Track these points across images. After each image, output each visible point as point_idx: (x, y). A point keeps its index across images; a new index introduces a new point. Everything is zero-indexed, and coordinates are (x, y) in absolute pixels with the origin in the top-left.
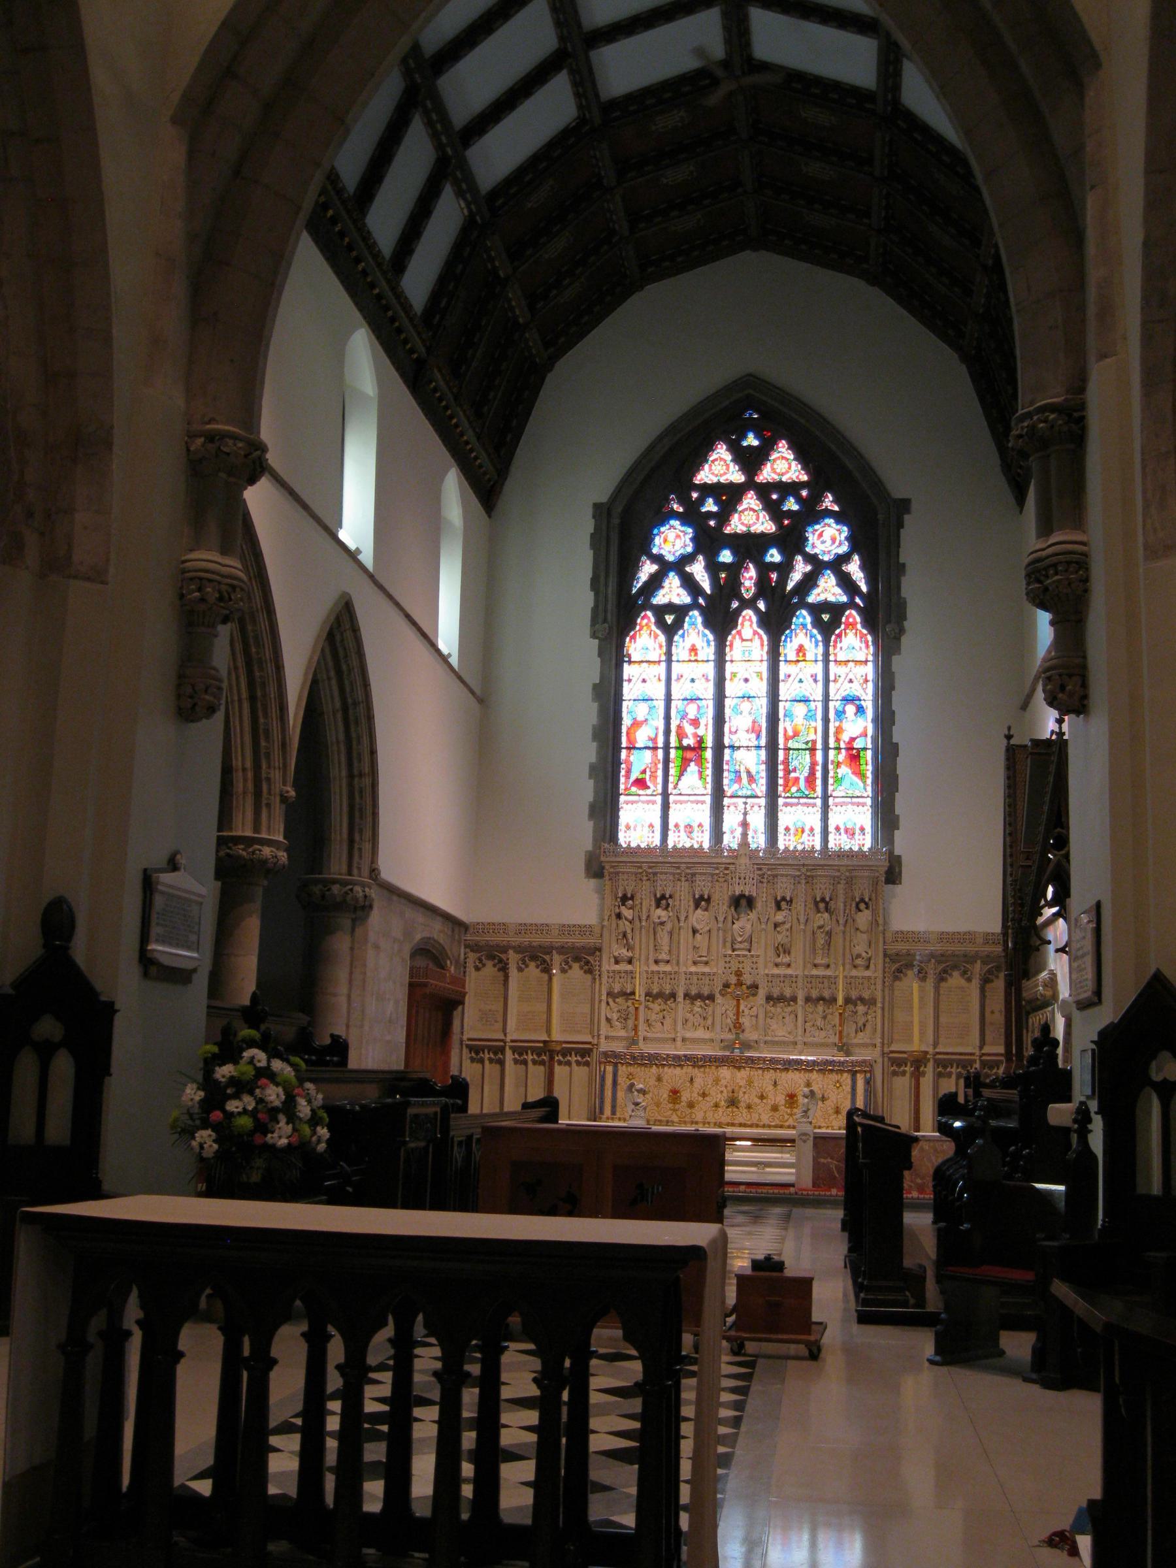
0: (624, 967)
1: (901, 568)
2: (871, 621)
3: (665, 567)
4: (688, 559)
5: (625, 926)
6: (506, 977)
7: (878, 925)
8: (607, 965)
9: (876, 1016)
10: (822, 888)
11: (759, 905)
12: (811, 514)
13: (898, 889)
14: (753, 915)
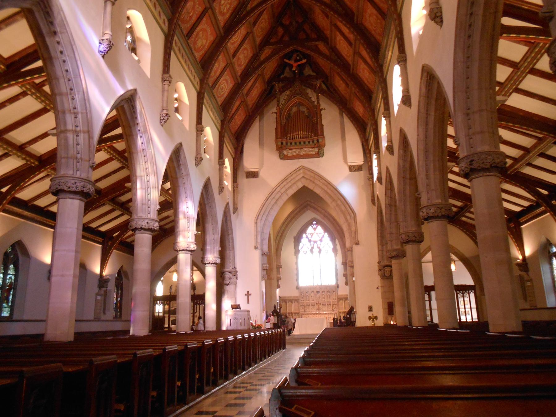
0: (302, 302)
5: (302, 296)
6: (286, 304)
8: (300, 302)
11: (320, 292)
13: (339, 289)
14: (319, 294)
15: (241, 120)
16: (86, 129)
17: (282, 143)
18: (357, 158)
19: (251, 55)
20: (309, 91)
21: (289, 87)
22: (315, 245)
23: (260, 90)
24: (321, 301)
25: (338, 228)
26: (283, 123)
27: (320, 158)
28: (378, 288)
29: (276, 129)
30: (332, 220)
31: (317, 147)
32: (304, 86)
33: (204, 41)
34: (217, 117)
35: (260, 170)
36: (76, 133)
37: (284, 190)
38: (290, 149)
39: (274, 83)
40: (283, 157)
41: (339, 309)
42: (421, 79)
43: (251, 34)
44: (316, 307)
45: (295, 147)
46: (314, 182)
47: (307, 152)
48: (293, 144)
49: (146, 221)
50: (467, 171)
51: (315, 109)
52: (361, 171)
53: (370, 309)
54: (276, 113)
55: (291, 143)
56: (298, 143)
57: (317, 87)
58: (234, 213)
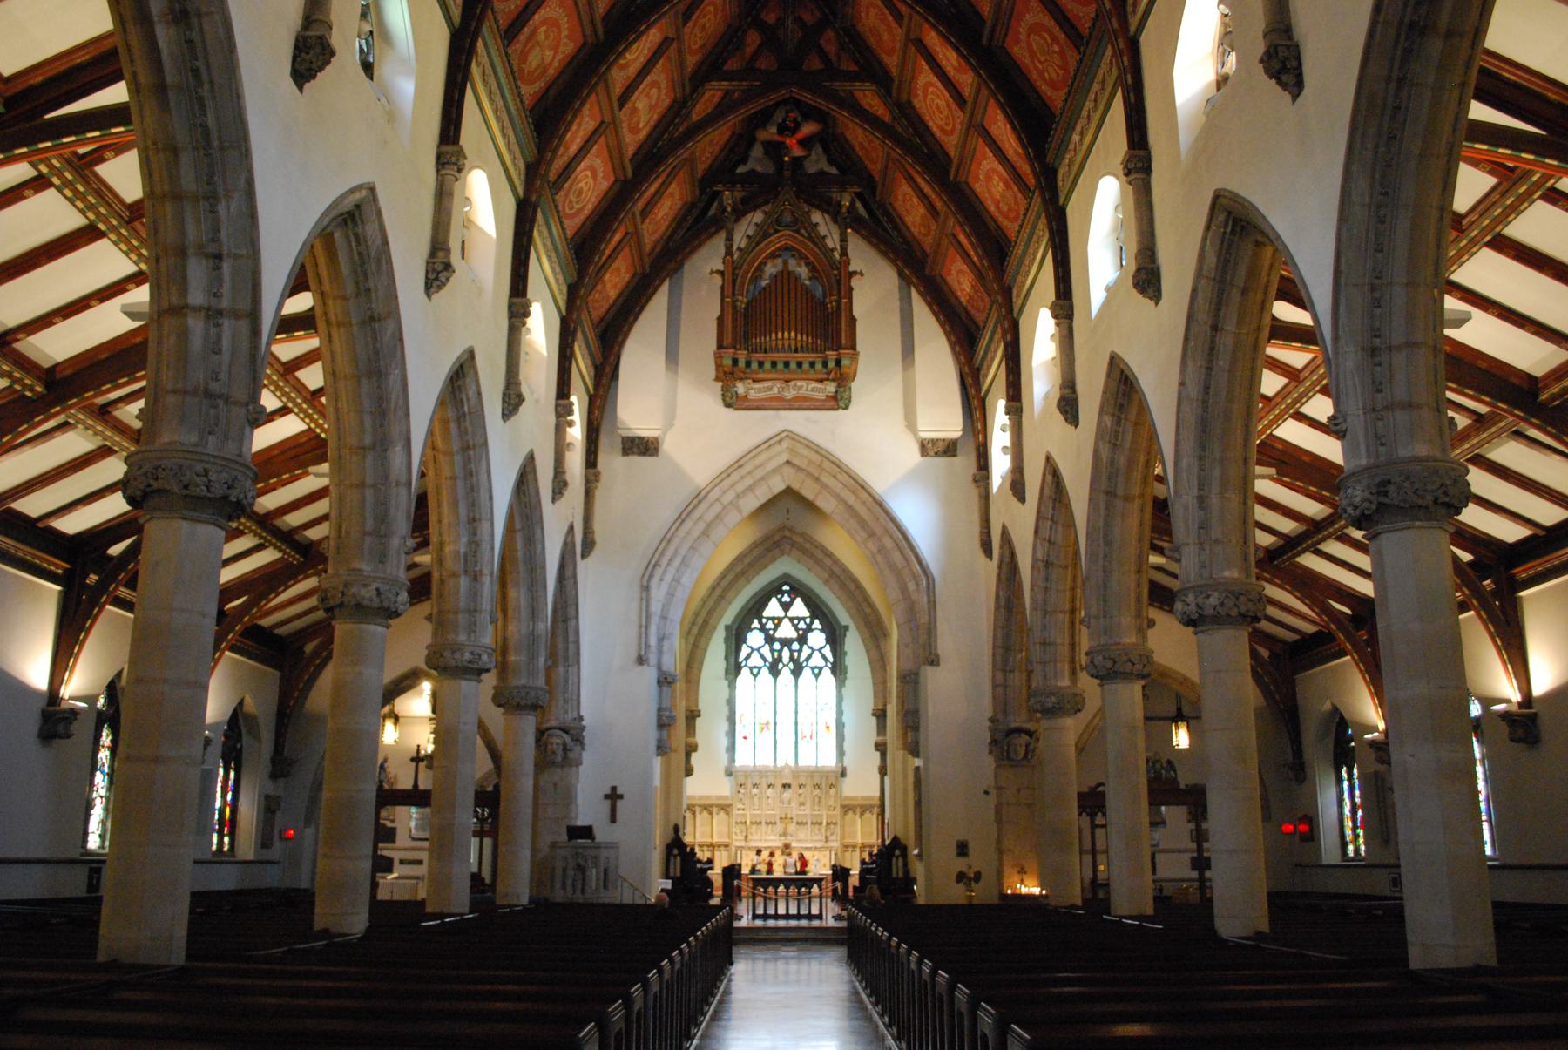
1: (845, 653)
2: (834, 671)
3: (753, 650)
4: (760, 648)
7: (838, 795)
8: (735, 812)
9: (838, 829)
10: (817, 781)
12: (809, 629)
14: (790, 791)
15: (619, 286)
16: (244, 305)
17: (735, 362)
18: (947, 421)
19: (666, 103)
20: (817, 217)
21: (761, 201)
22: (786, 654)
23: (679, 204)
24: (794, 812)
25: (868, 610)
26: (742, 302)
27: (841, 411)
28: (986, 793)
29: (720, 320)
30: (852, 587)
31: (833, 380)
32: (806, 202)
33: (549, 54)
34: (561, 278)
35: (665, 434)
36: (213, 314)
37: (730, 496)
38: (754, 381)
39: (719, 187)
40: (732, 401)
41: (843, 837)
42: (1208, 228)
43: (675, 44)
44: (780, 827)
45: (770, 376)
46: (817, 479)
47: (803, 392)
48: (767, 365)
49: (374, 586)
50: (1368, 509)
51: (835, 272)
52: (955, 456)
53: (962, 849)
54: (721, 273)
55: (761, 364)
56: (780, 366)
57: (844, 210)
58: (583, 556)
